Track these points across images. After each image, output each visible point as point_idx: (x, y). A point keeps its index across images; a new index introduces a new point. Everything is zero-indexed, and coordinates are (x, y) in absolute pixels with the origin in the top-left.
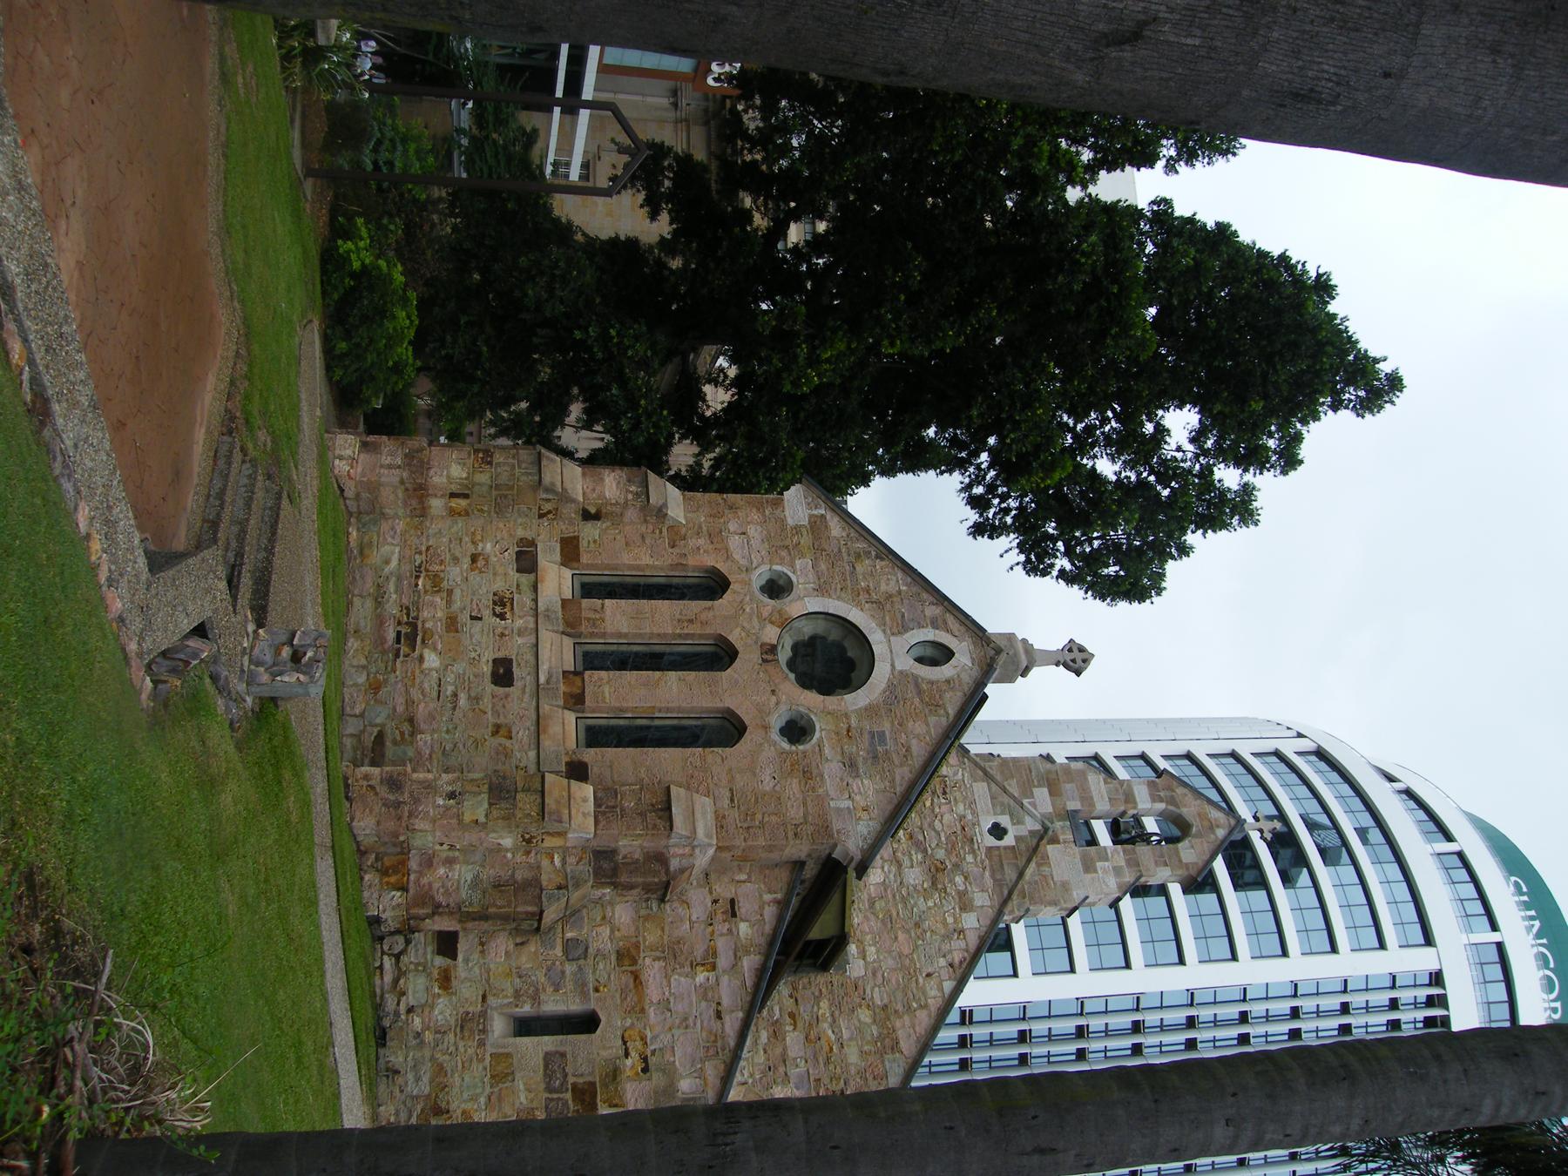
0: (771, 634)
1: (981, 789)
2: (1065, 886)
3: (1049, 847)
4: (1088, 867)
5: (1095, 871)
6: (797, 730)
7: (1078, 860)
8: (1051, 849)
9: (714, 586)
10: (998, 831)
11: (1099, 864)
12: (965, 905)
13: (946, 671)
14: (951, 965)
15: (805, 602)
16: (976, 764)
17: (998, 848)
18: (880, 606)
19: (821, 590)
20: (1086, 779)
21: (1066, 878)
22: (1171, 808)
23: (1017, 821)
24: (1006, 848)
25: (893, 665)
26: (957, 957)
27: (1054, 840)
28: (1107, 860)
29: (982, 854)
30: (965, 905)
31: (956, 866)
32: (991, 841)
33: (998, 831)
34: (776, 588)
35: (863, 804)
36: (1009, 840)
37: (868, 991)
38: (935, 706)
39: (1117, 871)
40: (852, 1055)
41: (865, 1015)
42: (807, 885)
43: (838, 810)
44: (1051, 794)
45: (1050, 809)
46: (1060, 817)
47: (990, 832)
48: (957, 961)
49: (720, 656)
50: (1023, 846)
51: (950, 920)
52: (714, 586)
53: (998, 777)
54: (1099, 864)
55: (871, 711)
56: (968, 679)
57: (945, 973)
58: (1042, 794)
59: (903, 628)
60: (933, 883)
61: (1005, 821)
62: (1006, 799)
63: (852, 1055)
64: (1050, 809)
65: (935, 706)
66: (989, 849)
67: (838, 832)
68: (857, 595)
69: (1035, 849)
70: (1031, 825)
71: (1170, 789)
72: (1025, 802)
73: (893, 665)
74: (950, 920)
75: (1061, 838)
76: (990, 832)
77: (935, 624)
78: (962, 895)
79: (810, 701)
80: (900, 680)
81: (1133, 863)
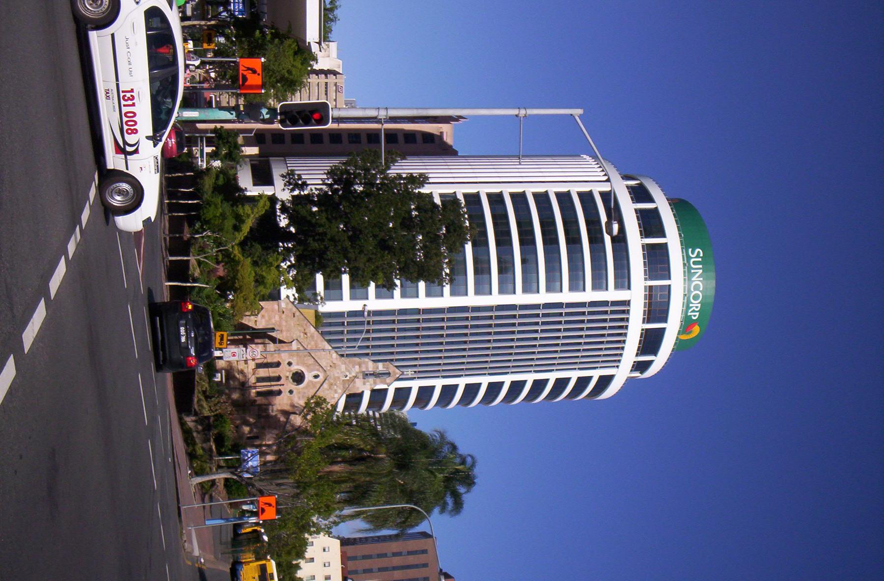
0: (288, 374)
1: (343, 367)
4: (364, 384)
6: (291, 392)
8: (357, 380)
9: (278, 364)
12: (336, 392)
13: (318, 380)
15: (295, 368)
18: (308, 366)
19: (298, 364)
30: (336, 392)
34: (290, 364)
38: (315, 387)
49: (278, 378)
52: (278, 364)
55: (303, 388)
58: (357, 367)
59: (312, 370)
61: (347, 374)
65: (315, 387)
68: (304, 364)
77: (318, 370)
79: (292, 386)
80: (310, 381)
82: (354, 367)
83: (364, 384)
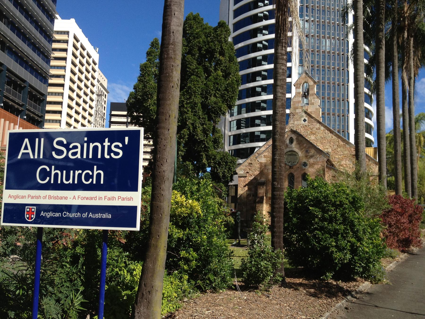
2: (317, 109)
4: (313, 104)
8: (309, 111)
10: (305, 120)
23: (303, 116)
27: (307, 110)
31: (311, 129)
32: (307, 122)
33: (305, 120)
36: (307, 119)
39: (314, 98)
40: (346, 152)
41: (339, 149)
58: (297, 111)
61: (303, 119)
63: (346, 152)
70: (304, 114)
78: (317, 129)
81: (313, 95)
83: (313, 104)
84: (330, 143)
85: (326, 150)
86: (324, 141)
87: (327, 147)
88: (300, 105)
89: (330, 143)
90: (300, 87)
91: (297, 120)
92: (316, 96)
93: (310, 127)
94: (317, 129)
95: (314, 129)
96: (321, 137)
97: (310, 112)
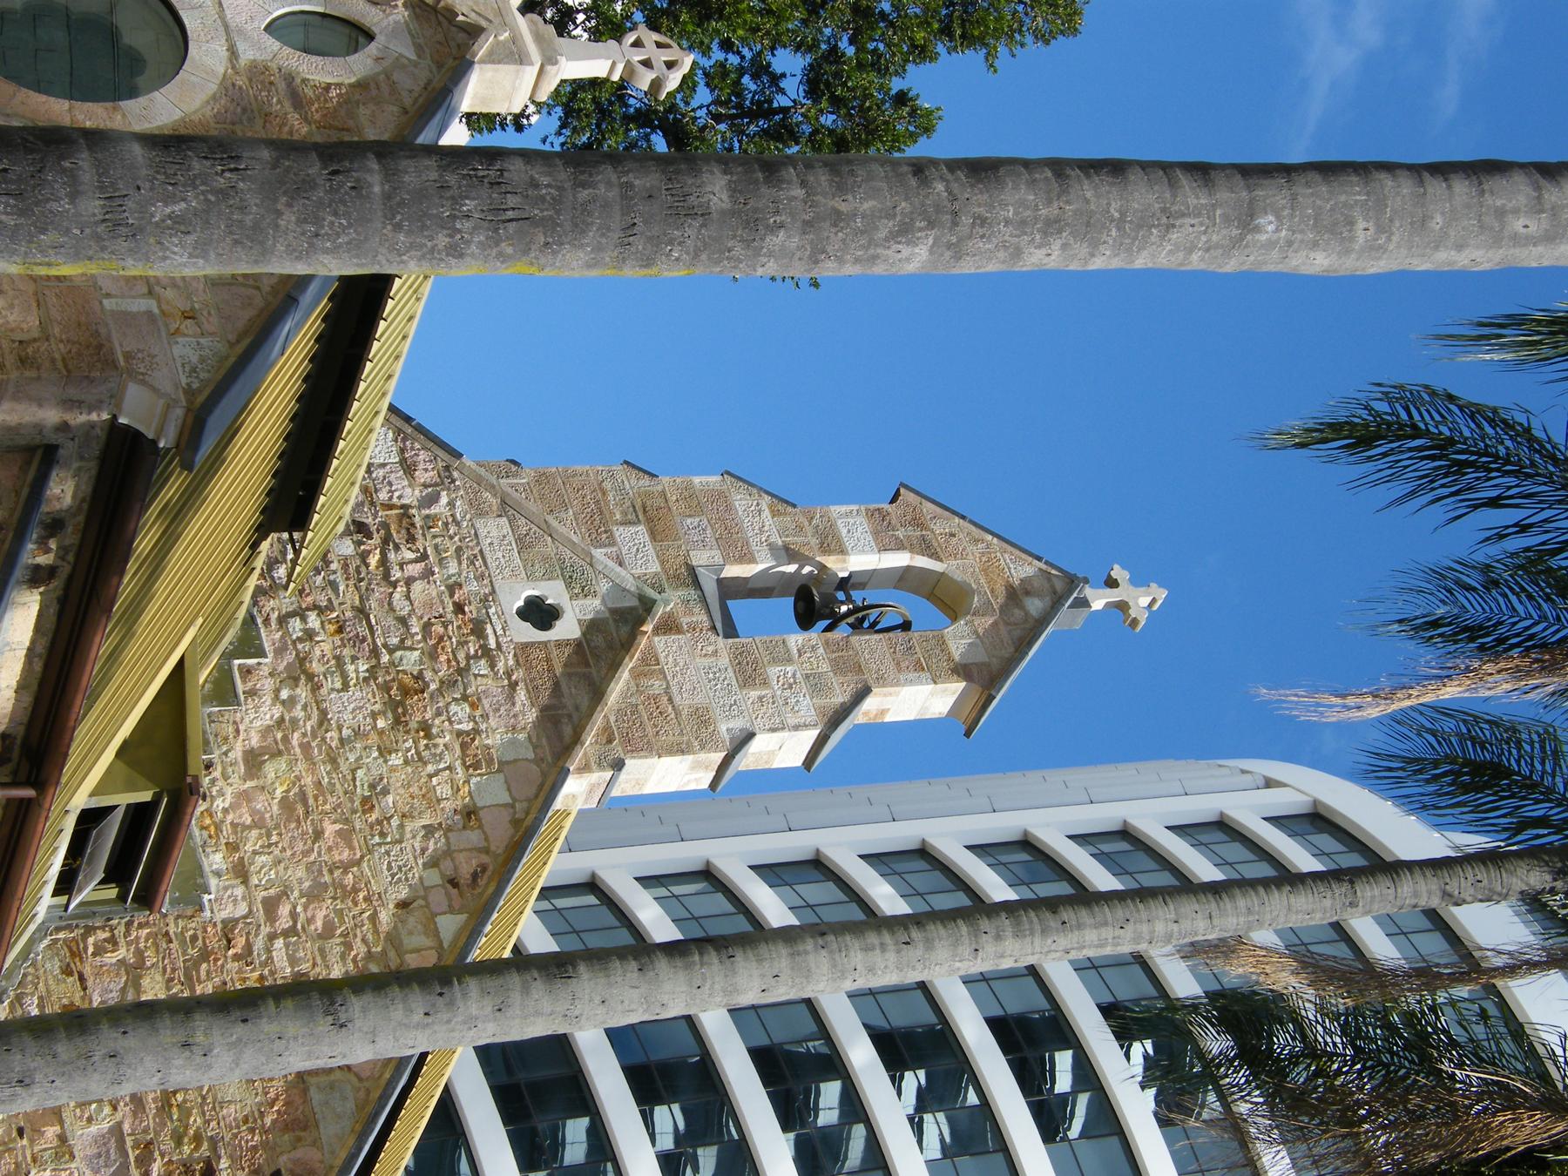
3: (660, 642)
5: (765, 683)
7: (724, 661)
11: (774, 671)
14: (453, 883)
16: (479, 480)
17: (545, 644)
20: (729, 508)
21: (699, 700)
22: (922, 562)
23: (579, 585)
24: (559, 644)
25: (233, 52)
26: (466, 868)
28: (789, 661)
29: (506, 661)
31: (447, 684)
32: (526, 632)
33: (540, 613)
35: (183, 305)
37: (259, 944)
39: (816, 684)
42: (71, 536)
43: (125, 318)
44: (653, 535)
45: (655, 567)
46: (676, 580)
47: (524, 614)
48: (466, 871)
50: (599, 640)
51: (444, 791)
53: (533, 507)
54: (774, 671)
56: (410, 85)
57: (438, 899)
58: (632, 538)
60: (397, 721)
61: (553, 592)
62: (549, 547)
64: (655, 567)
66: (525, 647)
67: (128, 356)
69: (628, 645)
71: (917, 522)
72: (598, 553)
73: (233, 52)
74: (444, 791)
75: (685, 621)
76: (524, 614)
82: (599, 529)
84: (313, 896)
85: (216, 860)
86: (330, 829)
87: (263, 871)
88: (700, 558)
89: (313, 896)
90: (900, 546)
91: (523, 544)
92: (840, 697)
93: (481, 667)
94: (466, 740)
95: (461, 711)
96: (378, 789)
97: (651, 658)
